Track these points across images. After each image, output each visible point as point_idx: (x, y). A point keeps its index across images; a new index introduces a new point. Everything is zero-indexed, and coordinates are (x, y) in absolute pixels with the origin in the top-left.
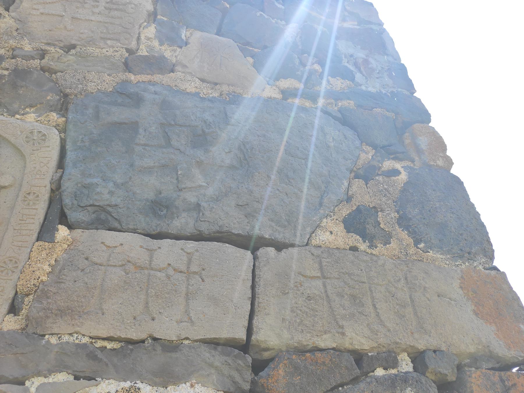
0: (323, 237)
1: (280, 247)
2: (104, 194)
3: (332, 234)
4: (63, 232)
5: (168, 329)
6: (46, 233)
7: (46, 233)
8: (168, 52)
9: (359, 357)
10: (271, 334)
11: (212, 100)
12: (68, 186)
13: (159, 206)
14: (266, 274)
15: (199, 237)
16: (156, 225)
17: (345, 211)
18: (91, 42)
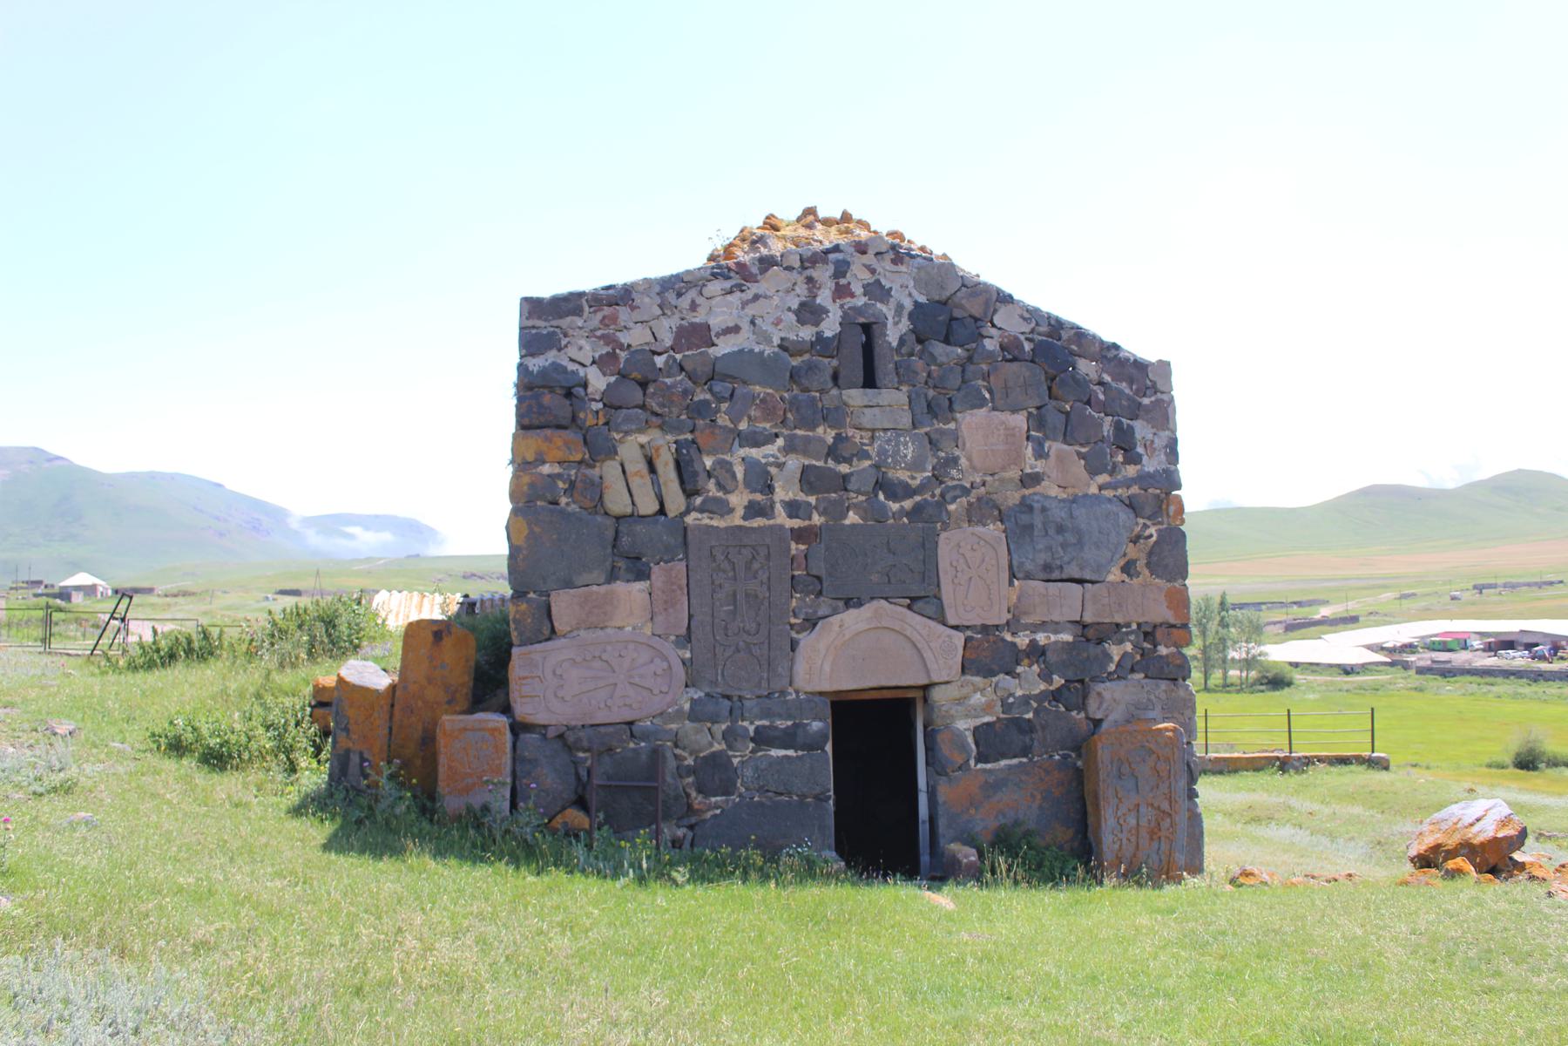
0: (1111, 578)
1: (1093, 582)
2: (1029, 566)
3: (1115, 575)
4: (1016, 582)
5: (1056, 618)
6: (1011, 584)
7: (1011, 584)
8: (1040, 466)
9: (1118, 625)
10: (1088, 619)
11: (1063, 501)
12: (1015, 563)
13: (1047, 567)
14: (1087, 596)
15: (1062, 581)
16: (1046, 577)
17: (1122, 563)
18: (1003, 469)
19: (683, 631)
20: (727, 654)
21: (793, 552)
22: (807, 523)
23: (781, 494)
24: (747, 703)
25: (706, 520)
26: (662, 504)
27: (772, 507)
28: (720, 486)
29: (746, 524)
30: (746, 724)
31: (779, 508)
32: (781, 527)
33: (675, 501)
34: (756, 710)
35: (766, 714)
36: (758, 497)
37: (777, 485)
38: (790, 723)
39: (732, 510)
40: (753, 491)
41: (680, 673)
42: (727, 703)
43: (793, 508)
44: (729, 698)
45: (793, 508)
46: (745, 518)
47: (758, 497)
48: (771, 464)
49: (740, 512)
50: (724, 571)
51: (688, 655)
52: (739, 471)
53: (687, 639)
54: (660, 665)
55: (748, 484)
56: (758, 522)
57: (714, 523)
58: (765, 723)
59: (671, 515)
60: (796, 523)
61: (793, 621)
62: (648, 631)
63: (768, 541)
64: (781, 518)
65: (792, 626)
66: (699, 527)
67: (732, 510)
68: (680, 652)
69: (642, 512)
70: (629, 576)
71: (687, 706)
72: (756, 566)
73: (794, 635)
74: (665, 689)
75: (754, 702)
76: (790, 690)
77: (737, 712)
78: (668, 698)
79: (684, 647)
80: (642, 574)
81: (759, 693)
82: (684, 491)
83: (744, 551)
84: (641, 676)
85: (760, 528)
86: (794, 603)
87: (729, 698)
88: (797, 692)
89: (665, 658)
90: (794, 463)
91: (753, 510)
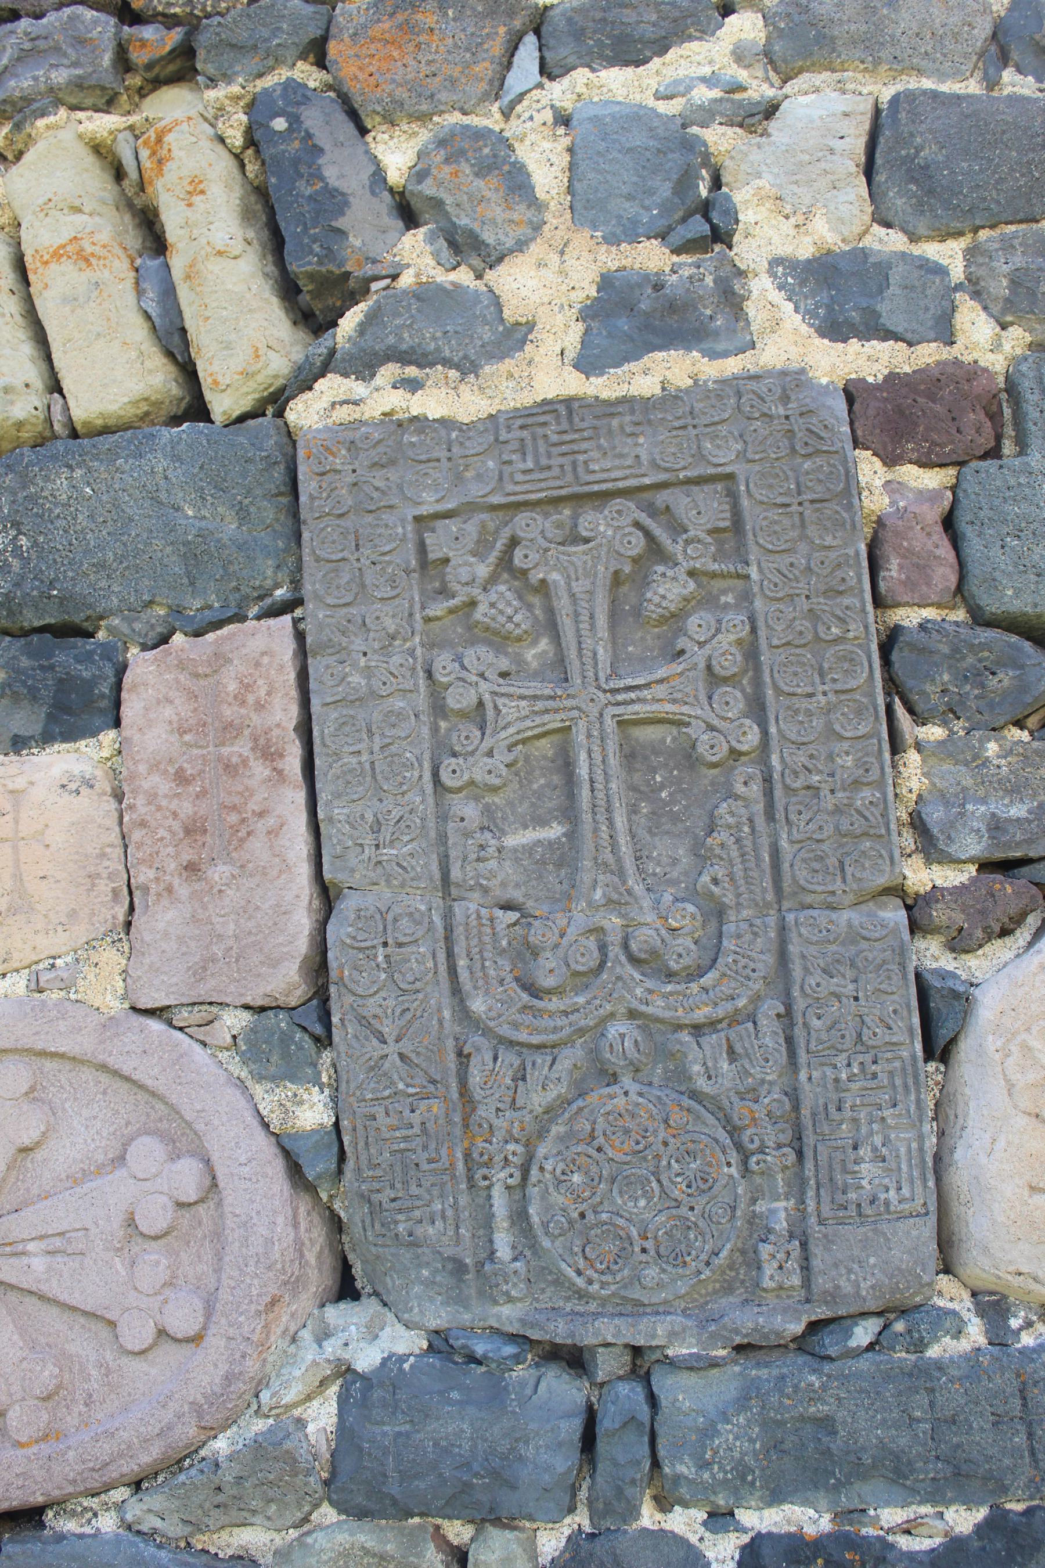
19: (286, 980)
20: (538, 1100)
21: (876, 501)
22: (929, 354)
23: (765, 236)
24: (679, 1392)
25: (381, 397)
26: (188, 372)
27: (731, 298)
28: (461, 245)
29: (602, 387)
30: (684, 1522)
31: (763, 294)
32: (792, 381)
33: (244, 335)
34: (736, 1439)
35: (803, 1459)
36: (652, 257)
37: (749, 203)
38: (964, 1519)
39: (515, 337)
40: (628, 233)
41: (266, 1214)
42: (563, 1390)
43: (839, 292)
44: (574, 1359)
45: (839, 292)
46: (587, 363)
47: (652, 257)
48: (706, 115)
49: (561, 334)
50: (498, 639)
51: (313, 1113)
52: (544, 161)
53: (310, 1020)
54: (159, 1180)
55: (585, 204)
56: (662, 372)
57: (432, 403)
58: (808, 1518)
59: (223, 405)
60: (871, 360)
61: (920, 876)
62: (104, 989)
63: (724, 455)
64: (784, 338)
65: (918, 913)
66: (350, 438)
67: (515, 337)
68: (268, 1099)
69: (80, 413)
70: (26, 720)
71: (322, 1417)
72: (669, 589)
73: (932, 954)
74: (183, 1319)
75: (724, 1385)
76: (951, 1295)
77: (621, 1450)
78: (206, 1370)
79: (292, 1071)
80: (81, 707)
81: (747, 1322)
82: (288, 289)
83: (597, 522)
84: (61, 1245)
85: (670, 398)
86: (914, 774)
87: (574, 1359)
88: (993, 1307)
89: (183, 1139)
90: (826, 110)
91: (627, 321)
